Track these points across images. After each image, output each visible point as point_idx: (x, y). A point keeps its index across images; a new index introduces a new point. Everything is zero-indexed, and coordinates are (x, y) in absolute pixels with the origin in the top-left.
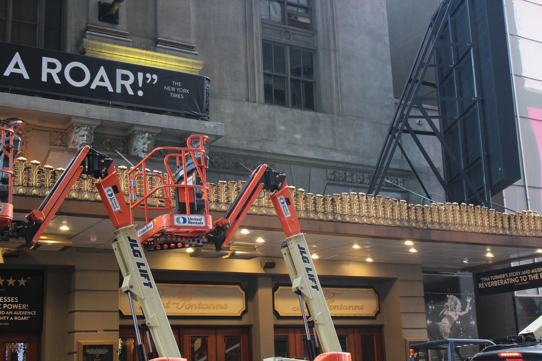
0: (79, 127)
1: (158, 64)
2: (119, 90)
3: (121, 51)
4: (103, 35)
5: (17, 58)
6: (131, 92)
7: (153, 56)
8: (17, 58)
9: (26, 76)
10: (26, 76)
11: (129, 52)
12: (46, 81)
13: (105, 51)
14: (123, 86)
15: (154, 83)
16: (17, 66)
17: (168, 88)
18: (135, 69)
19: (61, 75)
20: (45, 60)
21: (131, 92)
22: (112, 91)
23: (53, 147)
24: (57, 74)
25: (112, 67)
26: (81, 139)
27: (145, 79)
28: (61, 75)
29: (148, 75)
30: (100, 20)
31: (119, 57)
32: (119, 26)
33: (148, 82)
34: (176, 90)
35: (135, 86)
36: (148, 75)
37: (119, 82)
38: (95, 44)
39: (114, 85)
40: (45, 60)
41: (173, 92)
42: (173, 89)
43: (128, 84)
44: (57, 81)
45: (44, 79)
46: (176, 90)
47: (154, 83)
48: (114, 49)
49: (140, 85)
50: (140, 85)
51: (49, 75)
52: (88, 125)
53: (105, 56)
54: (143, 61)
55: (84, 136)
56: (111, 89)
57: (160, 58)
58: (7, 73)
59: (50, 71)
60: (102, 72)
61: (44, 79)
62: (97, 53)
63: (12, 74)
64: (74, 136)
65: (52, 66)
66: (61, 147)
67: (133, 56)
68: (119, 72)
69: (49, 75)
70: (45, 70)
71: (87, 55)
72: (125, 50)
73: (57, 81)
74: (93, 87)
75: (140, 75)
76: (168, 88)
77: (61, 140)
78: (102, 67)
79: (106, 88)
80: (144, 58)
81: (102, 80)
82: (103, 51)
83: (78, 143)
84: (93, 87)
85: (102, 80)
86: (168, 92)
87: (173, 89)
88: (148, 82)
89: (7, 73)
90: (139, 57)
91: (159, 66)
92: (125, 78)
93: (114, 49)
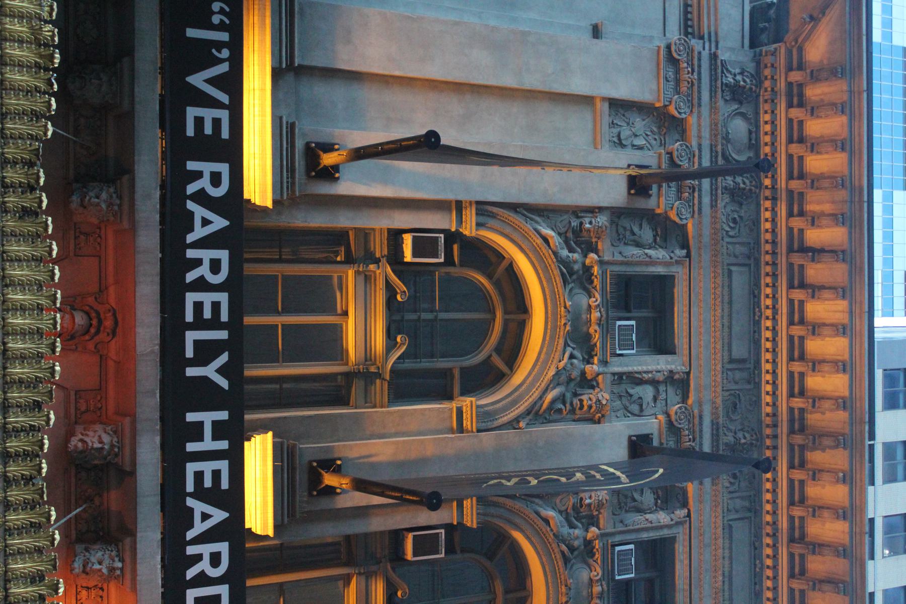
0: (115, 432)
12: (188, 420)
16: (205, 517)
22: (188, 538)
23: (73, 397)
24: (203, 572)
26: (95, 440)
37: (206, 549)
39: (201, 539)
52: (121, 448)
55: (101, 442)
59: (206, 558)
64: (99, 427)
66: (73, 411)
77: (87, 411)
79: (191, 526)
83: (87, 435)
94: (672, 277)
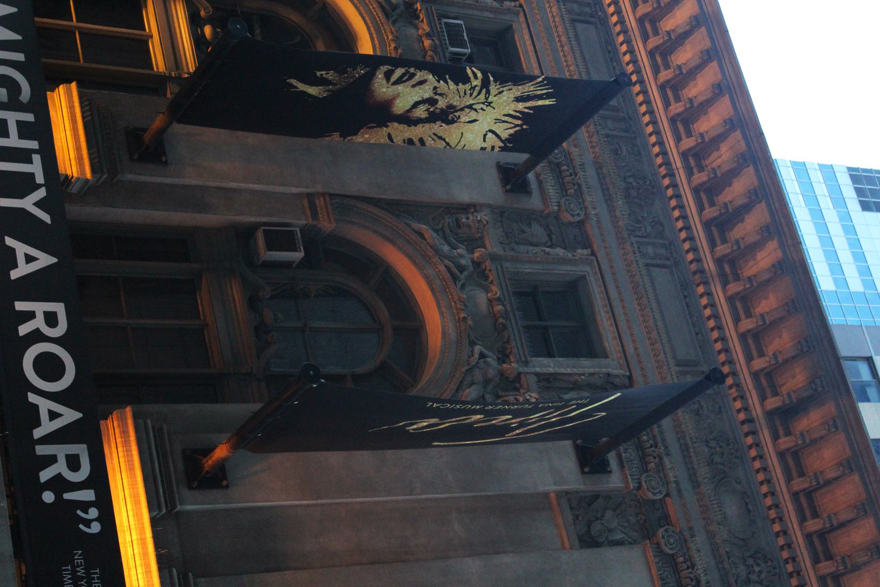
1: (133, 572)
2: (42, 450)
3: (133, 485)
4: (154, 452)
5: (45, 260)
6: (45, 475)
7: (145, 554)
8: (45, 260)
9: (14, 274)
10: (14, 274)
11: (137, 502)
13: (121, 454)
14: (52, 460)
15: (81, 526)
17: (78, 559)
18: (99, 481)
19: (37, 336)
20: (59, 308)
21: (45, 475)
25: (87, 432)
27: (85, 506)
28: (37, 336)
29: (93, 513)
30: (184, 451)
31: (120, 487)
32: (186, 493)
33: (79, 512)
34: (82, 578)
35: (59, 484)
36: (93, 513)
38: (128, 432)
40: (59, 308)
41: (74, 572)
42: (81, 572)
43: (60, 467)
44: (24, 329)
45: (20, 306)
46: (82, 578)
47: (81, 526)
48: (131, 469)
49: (67, 496)
50: (67, 496)
51: (31, 315)
53: (112, 459)
54: (128, 539)
56: (38, 433)
57: (148, 572)
58: (9, 241)
60: (70, 415)
61: (20, 306)
62: (115, 455)
63: (13, 250)
65: (51, 319)
67: (130, 513)
68: (81, 450)
69: (31, 315)
70: (40, 308)
71: (102, 422)
72: (138, 494)
73: (24, 329)
74: (32, 398)
75: (88, 495)
76: (78, 559)
78: (80, 415)
80: (134, 537)
81: (53, 415)
82: (120, 449)
84: (32, 398)
85: (53, 415)
86: (71, 562)
87: (81, 572)
88: (79, 512)
89: (9, 241)
90: (133, 527)
91: (130, 575)
92: (73, 463)
93: (128, 451)
94: (509, 29)
